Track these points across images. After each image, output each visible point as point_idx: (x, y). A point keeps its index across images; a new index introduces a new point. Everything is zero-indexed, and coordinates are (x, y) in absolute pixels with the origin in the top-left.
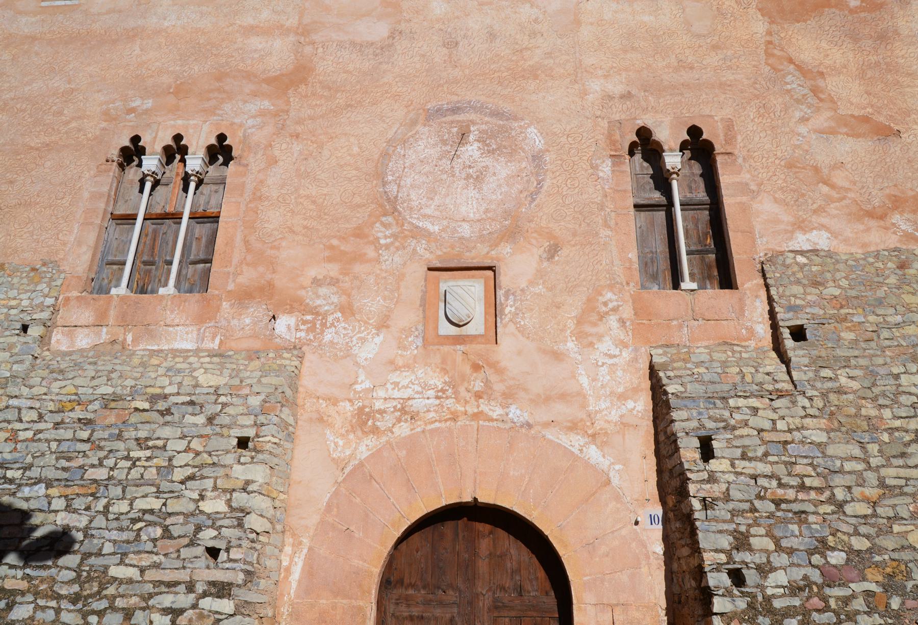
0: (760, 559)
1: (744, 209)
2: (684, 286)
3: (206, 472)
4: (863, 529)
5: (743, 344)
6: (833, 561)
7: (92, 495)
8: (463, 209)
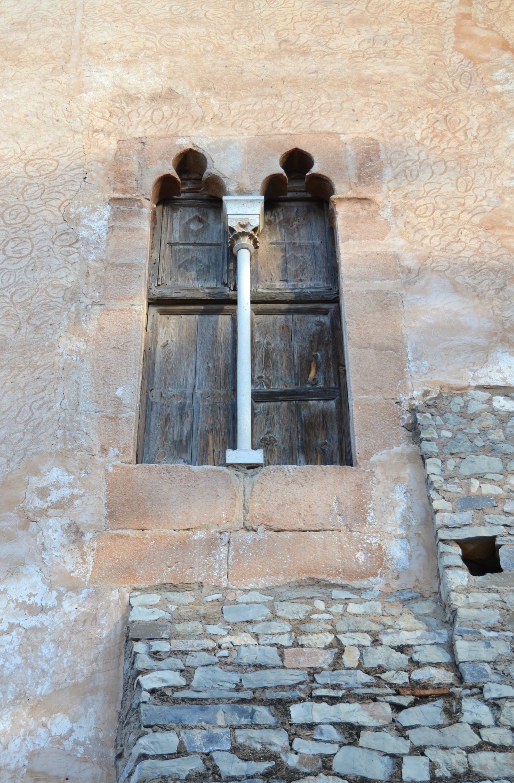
5: (356, 584)
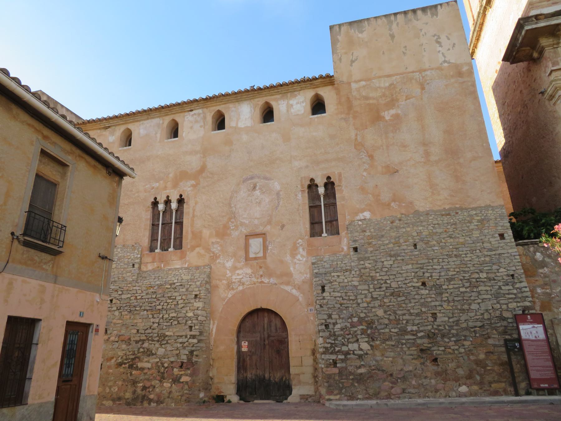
0: (334, 321)
2: (323, 235)
3: (188, 305)
6: (354, 321)
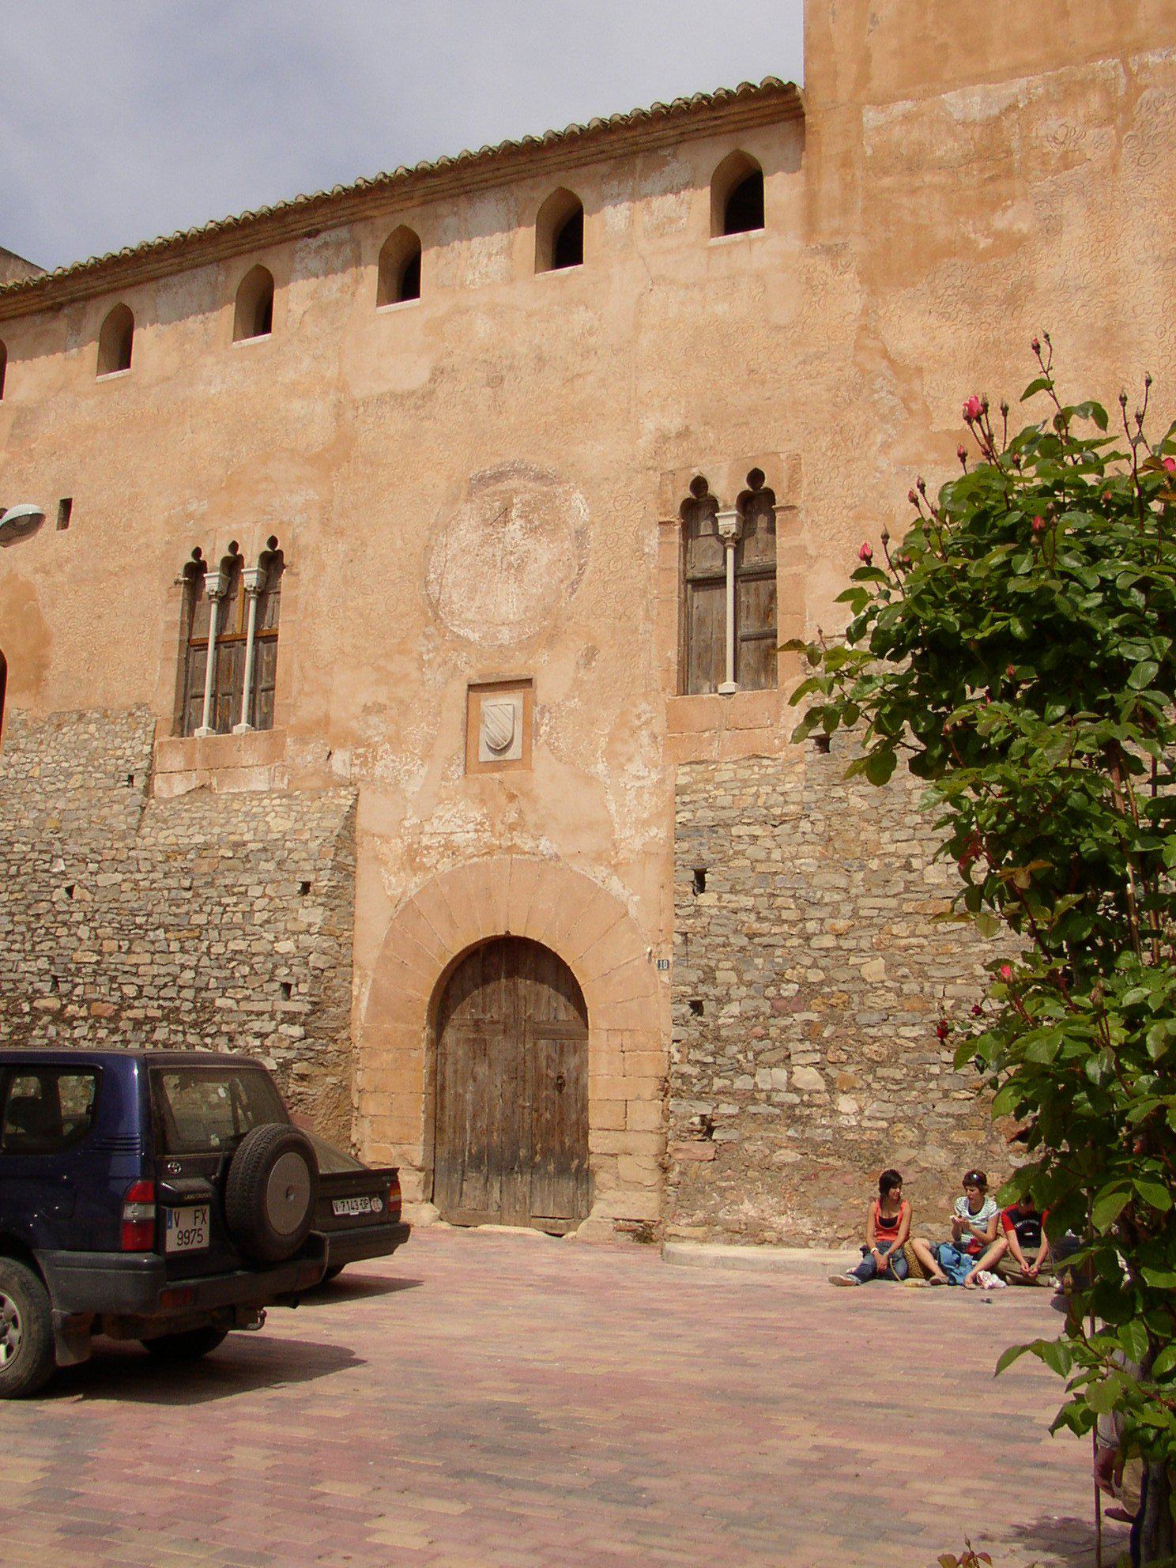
1: (798, 581)
4: (823, 963)
6: (785, 994)
7: (198, 938)
8: (504, 609)
